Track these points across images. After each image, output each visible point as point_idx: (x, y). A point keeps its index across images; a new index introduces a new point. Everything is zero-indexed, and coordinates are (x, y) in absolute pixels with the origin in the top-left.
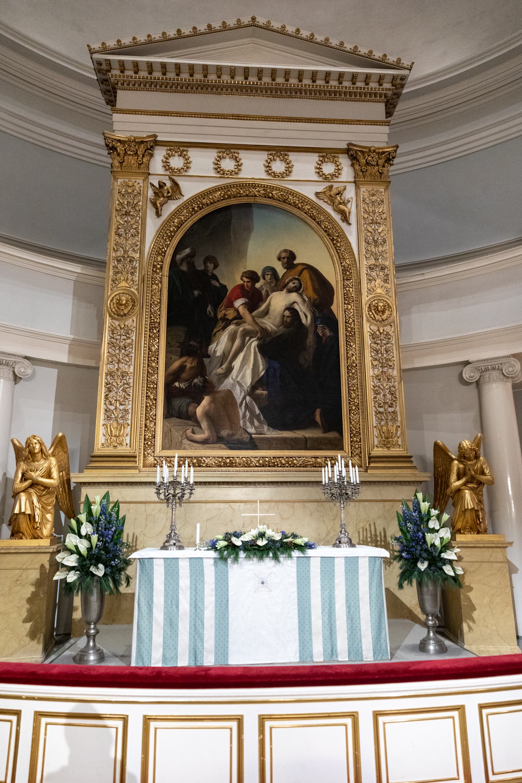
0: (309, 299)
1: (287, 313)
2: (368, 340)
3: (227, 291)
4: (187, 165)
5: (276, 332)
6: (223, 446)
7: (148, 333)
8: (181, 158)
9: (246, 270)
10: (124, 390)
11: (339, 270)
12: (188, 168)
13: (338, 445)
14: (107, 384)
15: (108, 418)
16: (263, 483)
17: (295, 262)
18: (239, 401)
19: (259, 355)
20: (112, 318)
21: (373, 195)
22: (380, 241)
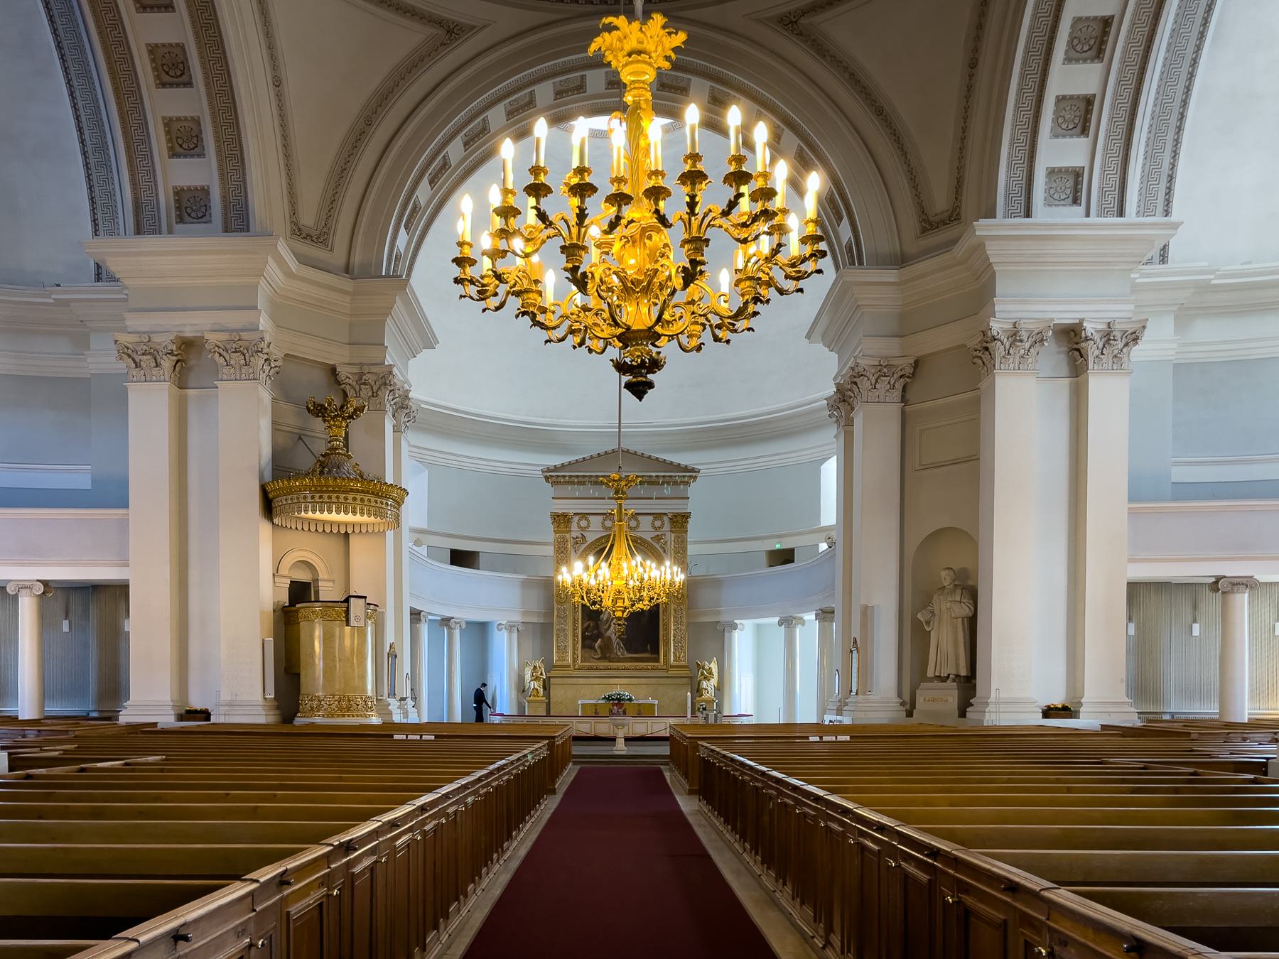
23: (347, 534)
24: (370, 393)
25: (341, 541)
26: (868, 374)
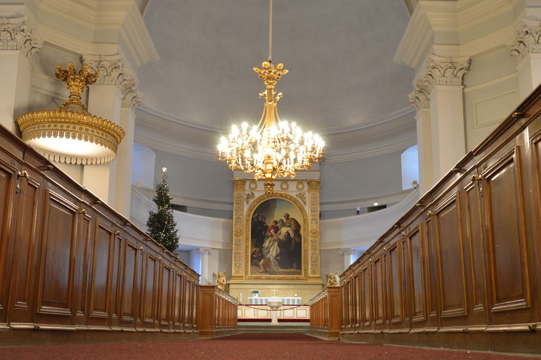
0: (293, 229)
1: (286, 234)
2: (310, 242)
3: (268, 227)
4: (256, 187)
5: (283, 240)
6: (267, 274)
7: (246, 241)
8: (254, 185)
9: (274, 221)
10: (239, 258)
11: (302, 220)
12: (257, 188)
13: (300, 273)
14: (235, 256)
15: (235, 266)
16: (278, 284)
17: (289, 218)
18: (272, 261)
19: (278, 247)
20: (235, 237)
21: (314, 195)
22: (315, 210)
24: (105, 74)
25: (79, 170)
26: (439, 67)
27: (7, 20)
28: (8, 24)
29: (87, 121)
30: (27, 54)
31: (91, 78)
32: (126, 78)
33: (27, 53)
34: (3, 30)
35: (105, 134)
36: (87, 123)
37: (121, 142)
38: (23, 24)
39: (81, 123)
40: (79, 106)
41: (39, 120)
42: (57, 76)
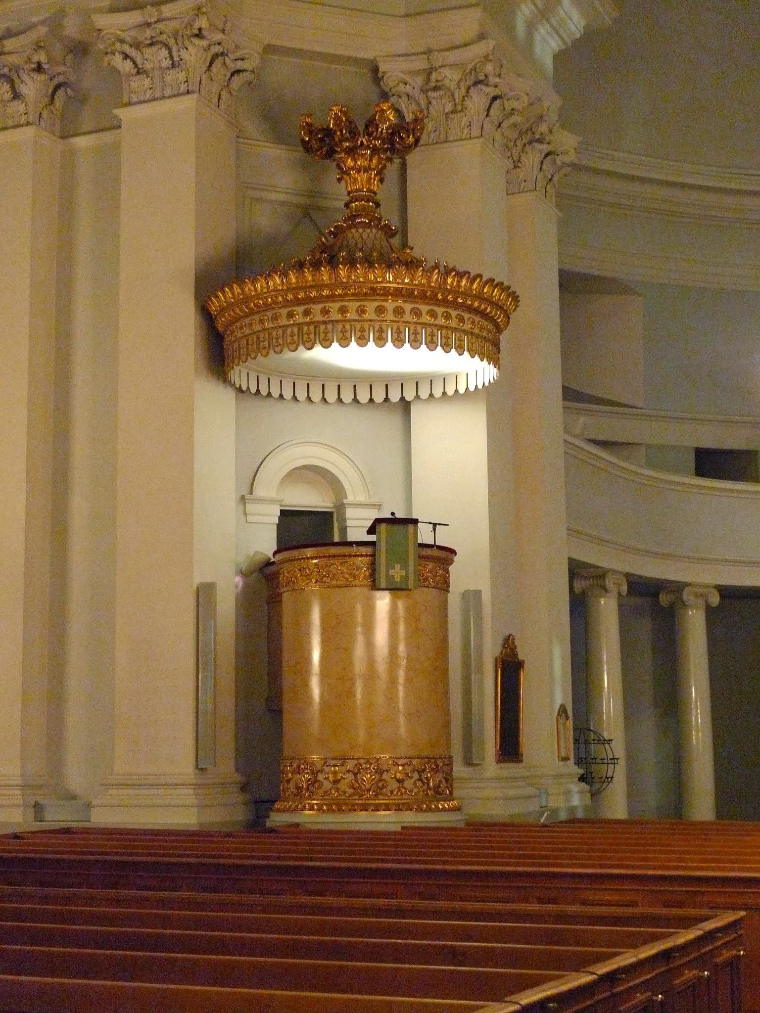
23: (405, 406)
27: (157, 11)
28: (158, 21)
29: (394, 285)
30: (219, 98)
31: (401, 138)
32: (515, 104)
33: (220, 95)
34: (148, 42)
35: (454, 313)
36: (396, 289)
37: (508, 322)
38: (197, 15)
39: (378, 295)
40: (374, 231)
41: (261, 301)
42: (307, 147)
